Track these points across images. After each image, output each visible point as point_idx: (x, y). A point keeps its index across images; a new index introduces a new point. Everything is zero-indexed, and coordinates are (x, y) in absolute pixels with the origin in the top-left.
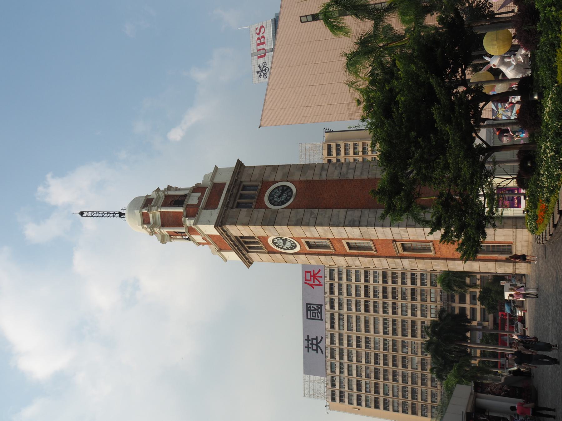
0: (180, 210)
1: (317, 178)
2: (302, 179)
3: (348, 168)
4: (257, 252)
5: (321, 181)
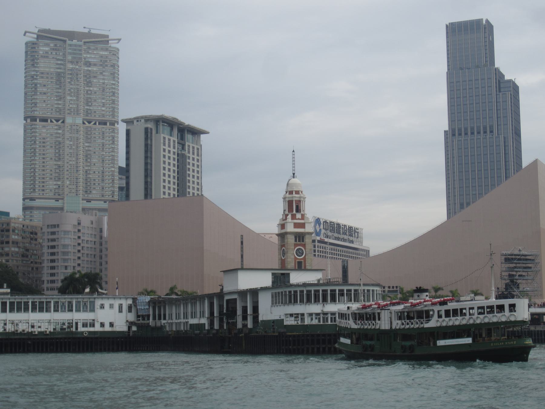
0: (294, 212)
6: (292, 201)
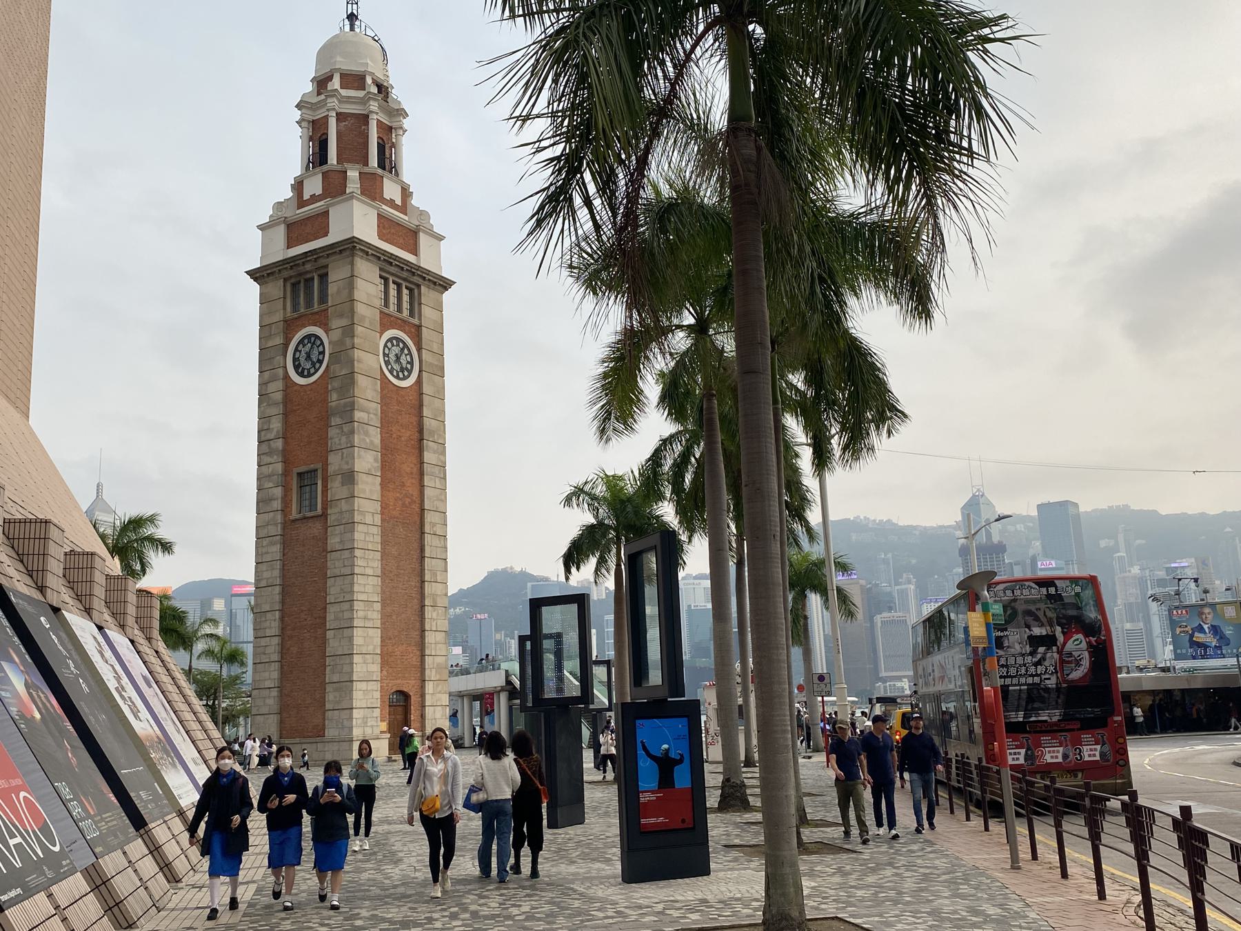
4: (285, 298)
6: (365, 119)
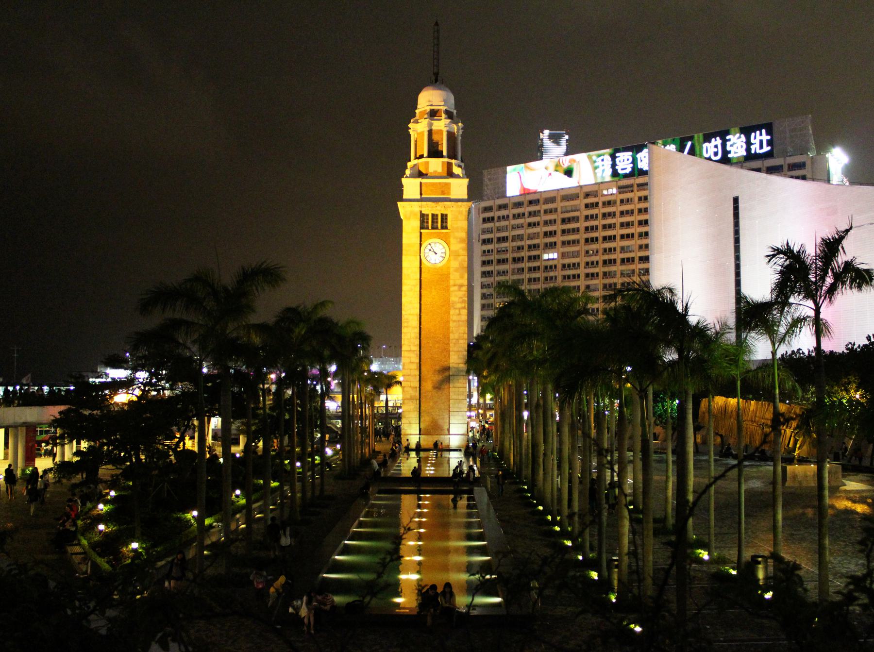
1: (452, 282)
2: (451, 270)
3: (459, 309)
5: (448, 286)
